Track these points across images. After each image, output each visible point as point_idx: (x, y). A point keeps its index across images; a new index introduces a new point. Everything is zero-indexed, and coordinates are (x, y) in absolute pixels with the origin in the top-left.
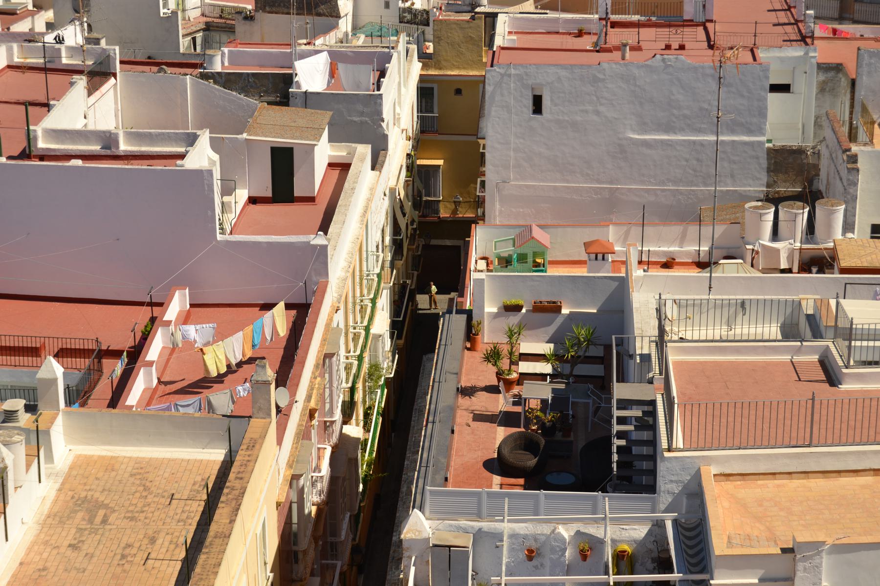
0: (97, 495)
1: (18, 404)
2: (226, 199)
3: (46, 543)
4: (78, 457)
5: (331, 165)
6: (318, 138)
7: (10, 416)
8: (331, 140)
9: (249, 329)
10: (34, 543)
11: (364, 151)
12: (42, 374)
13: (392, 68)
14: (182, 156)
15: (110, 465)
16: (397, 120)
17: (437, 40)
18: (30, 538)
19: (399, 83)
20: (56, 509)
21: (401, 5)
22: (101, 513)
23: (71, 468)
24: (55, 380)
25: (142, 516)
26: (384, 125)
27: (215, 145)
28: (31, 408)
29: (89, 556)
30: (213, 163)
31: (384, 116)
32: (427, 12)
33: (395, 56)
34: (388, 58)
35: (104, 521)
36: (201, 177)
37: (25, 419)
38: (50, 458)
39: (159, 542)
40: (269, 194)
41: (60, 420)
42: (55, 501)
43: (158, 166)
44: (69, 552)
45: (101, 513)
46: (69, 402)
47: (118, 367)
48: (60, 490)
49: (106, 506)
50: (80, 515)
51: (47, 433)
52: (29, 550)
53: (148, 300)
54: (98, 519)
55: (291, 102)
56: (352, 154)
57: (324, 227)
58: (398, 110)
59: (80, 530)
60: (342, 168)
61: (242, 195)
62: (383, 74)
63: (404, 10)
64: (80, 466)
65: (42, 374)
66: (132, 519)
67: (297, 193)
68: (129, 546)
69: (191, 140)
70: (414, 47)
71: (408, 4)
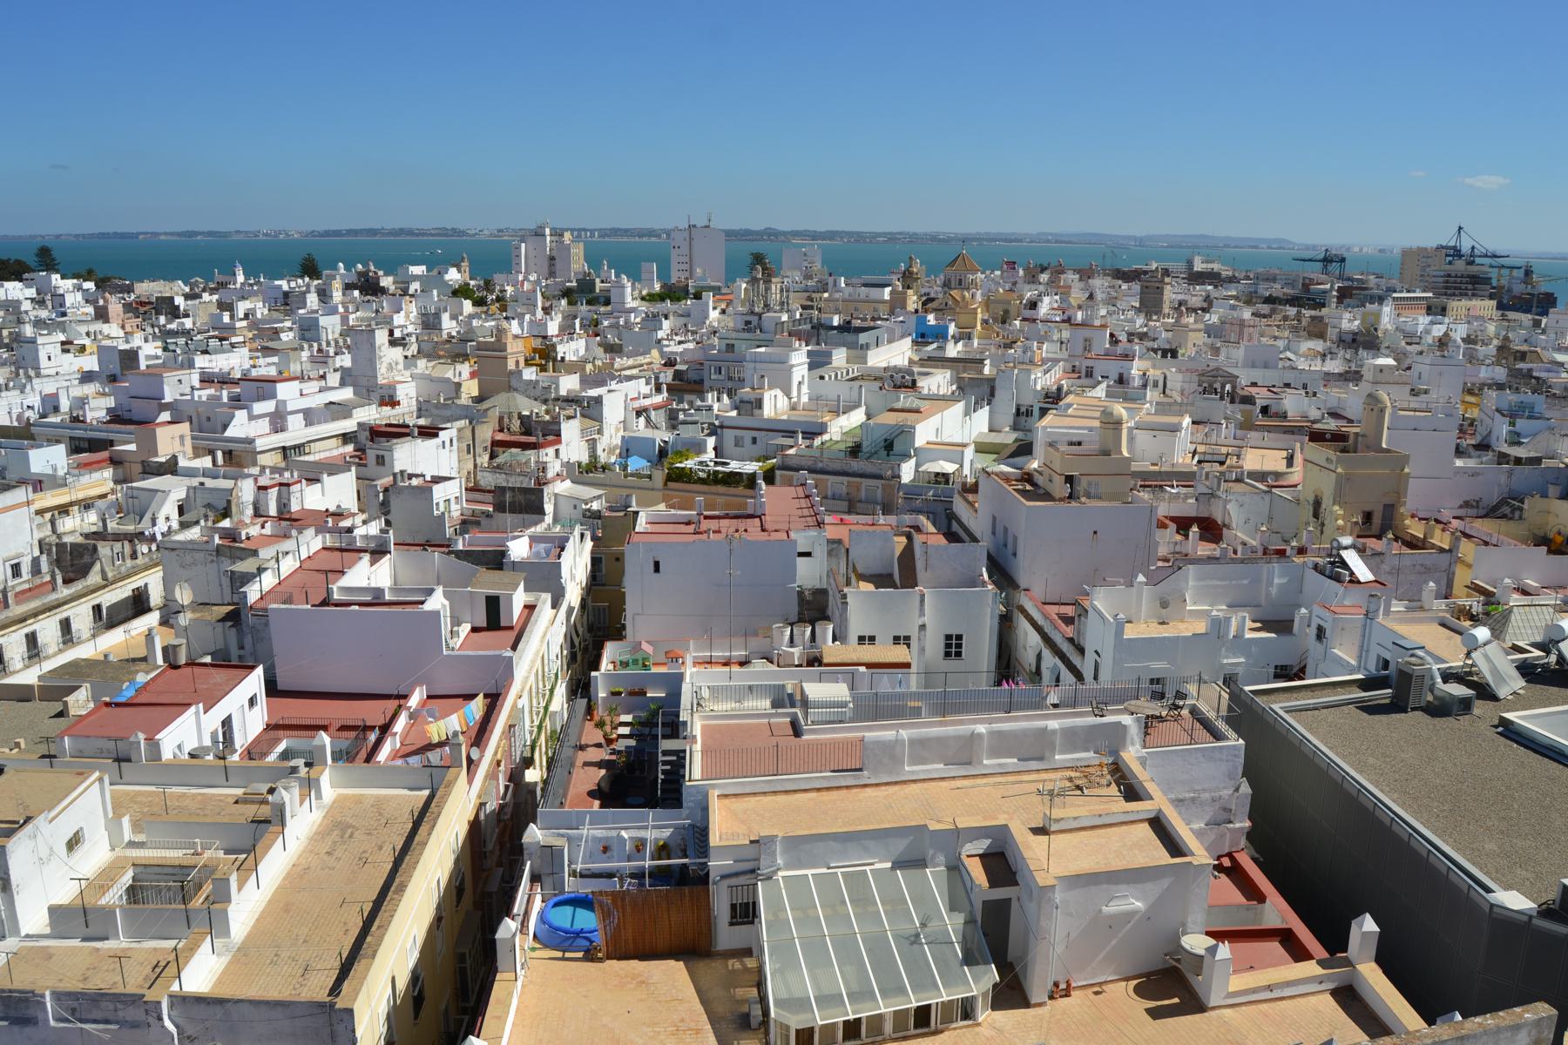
0: (348, 819)
1: (300, 762)
2: (455, 629)
3: (311, 851)
4: (339, 795)
5: (526, 607)
6: (515, 588)
7: (294, 770)
8: (526, 590)
9: (461, 712)
10: (304, 852)
11: (547, 598)
12: (316, 742)
13: (570, 546)
14: (422, 603)
15: (359, 800)
16: (573, 577)
17: (604, 528)
18: (301, 848)
19: (575, 555)
20: (320, 829)
21: (584, 507)
22: (349, 831)
23: (334, 803)
24: (325, 746)
25: (375, 832)
26: (563, 581)
27: (446, 595)
28: (309, 765)
29: (338, 859)
30: (444, 606)
31: (563, 575)
32: (599, 511)
33: (572, 538)
34: (567, 539)
35: (351, 836)
36: (436, 614)
37: (303, 771)
38: (319, 796)
39: (385, 849)
40: (485, 625)
41: (327, 771)
42: (320, 826)
43: (409, 609)
44: (326, 857)
45: (349, 831)
46: (333, 759)
47: (373, 737)
48: (325, 817)
49: (353, 827)
50: (335, 833)
51: (318, 780)
52: (300, 856)
53: (396, 693)
54: (347, 835)
55: (505, 567)
56: (537, 600)
57: (514, 648)
58: (574, 571)
59: (335, 843)
60: (530, 608)
61: (465, 628)
62: (563, 549)
63: (586, 510)
64: (339, 802)
65: (316, 742)
66: (369, 834)
67: (502, 624)
68: (364, 852)
69: (430, 592)
70: (588, 535)
71: (588, 507)
